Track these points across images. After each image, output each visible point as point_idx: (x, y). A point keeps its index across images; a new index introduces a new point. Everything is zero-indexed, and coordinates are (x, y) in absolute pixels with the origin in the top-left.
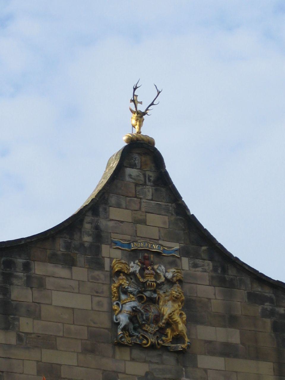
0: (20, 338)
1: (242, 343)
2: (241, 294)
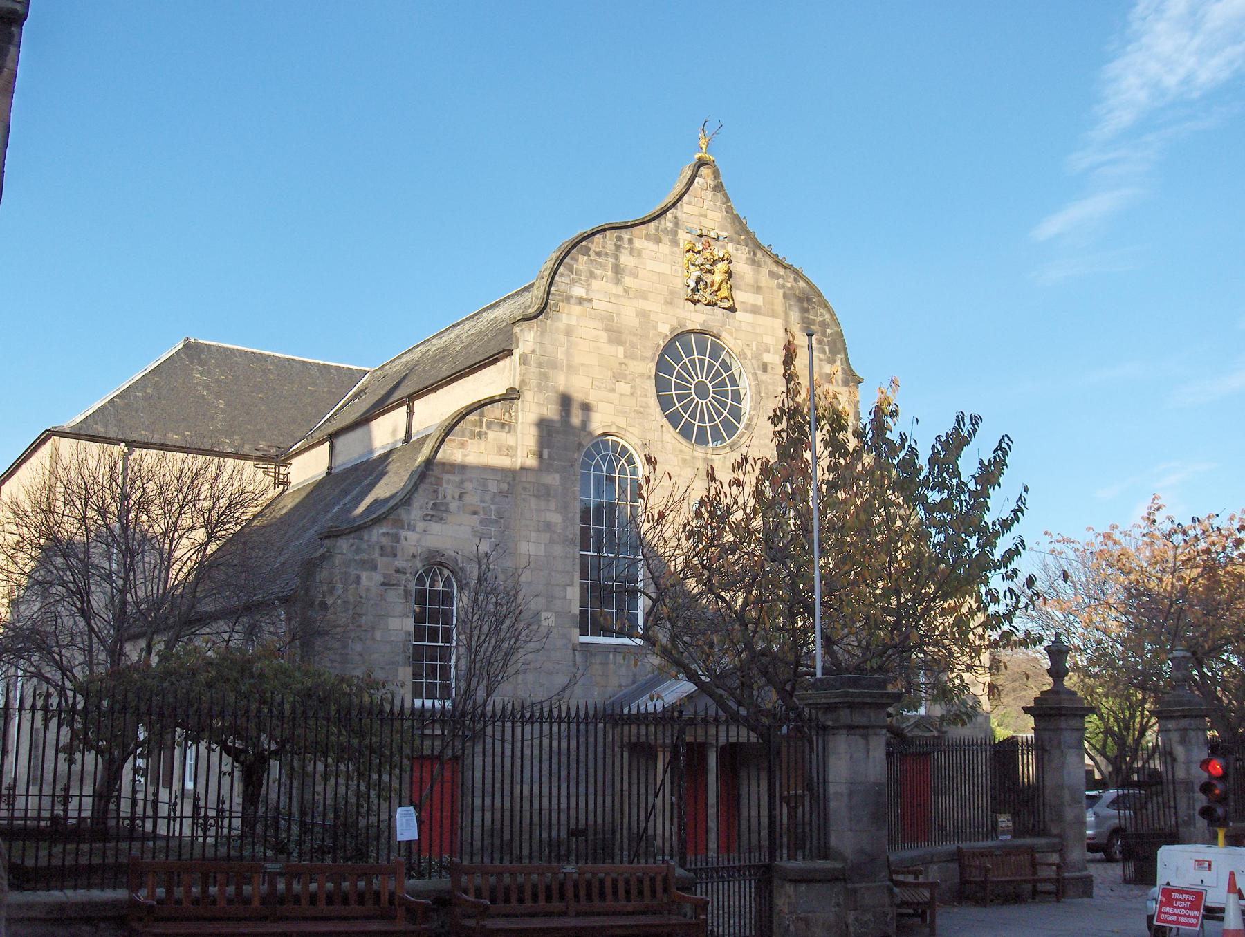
0: (626, 291)
2: (764, 271)
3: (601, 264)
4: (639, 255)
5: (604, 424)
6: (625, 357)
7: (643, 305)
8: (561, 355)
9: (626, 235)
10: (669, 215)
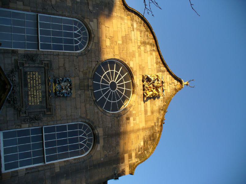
3: (145, 36)
4: (151, 54)
6: (119, 44)
7: (137, 54)
9: (155, 48)
10: (165, 68)
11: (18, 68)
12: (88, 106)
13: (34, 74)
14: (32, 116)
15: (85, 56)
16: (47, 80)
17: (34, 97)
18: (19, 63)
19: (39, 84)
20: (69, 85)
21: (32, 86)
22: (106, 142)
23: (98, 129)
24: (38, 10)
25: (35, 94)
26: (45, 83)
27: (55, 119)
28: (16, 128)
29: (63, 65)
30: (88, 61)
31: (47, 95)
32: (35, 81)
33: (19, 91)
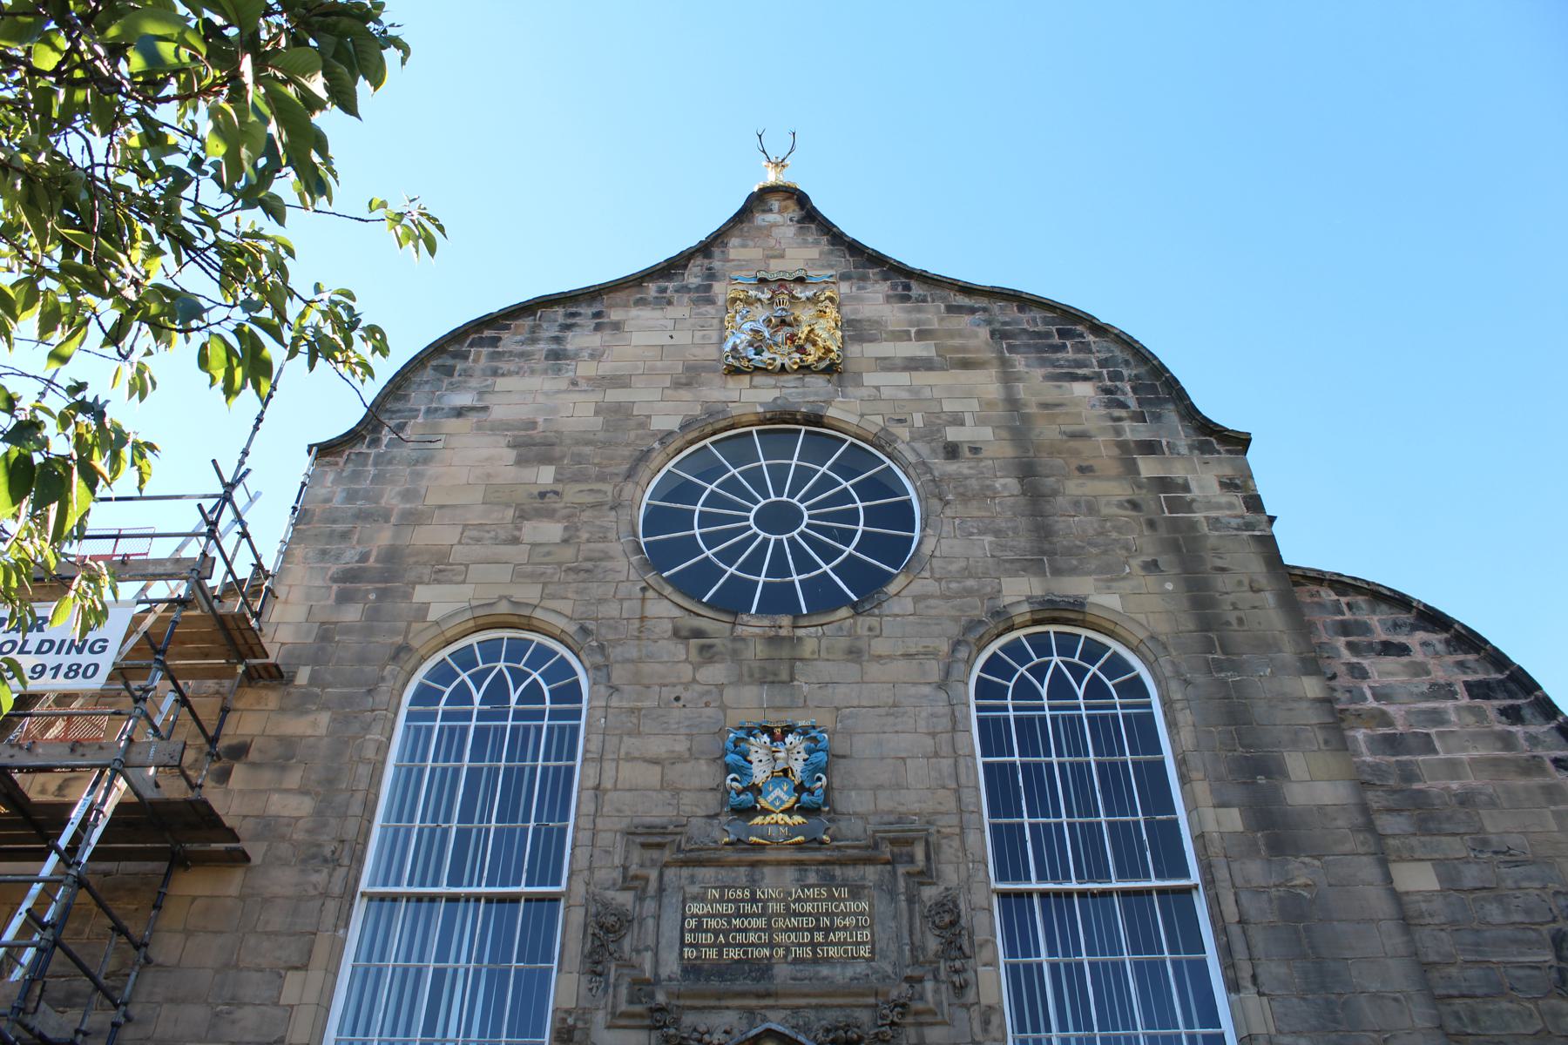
1: (938, 356)
5: (474, 603)
6: (556, 480)
7: (614, 396)
8: (391, 498)
9: (586, 310)
11: (661, 1009)
12: (880, 646)
13: (700, 923)
14: (933, 944)
15: (615, 653)
16: (734, 857)
17: (828, 931)
18: (631, 1002)
19: (753, 900)
20: (766, 738)
21: (765, 937)
22: (1075, 562)
23: (1007, 601)
24: (337, 889)
25: (812, 923)
26: (753, 865)
27: (954, 820)
28: (998, 1035)
29: (658, 769)
30: (638, 638)
31: (819, 856)
32: (736, 922)
33: (789, 1012)
